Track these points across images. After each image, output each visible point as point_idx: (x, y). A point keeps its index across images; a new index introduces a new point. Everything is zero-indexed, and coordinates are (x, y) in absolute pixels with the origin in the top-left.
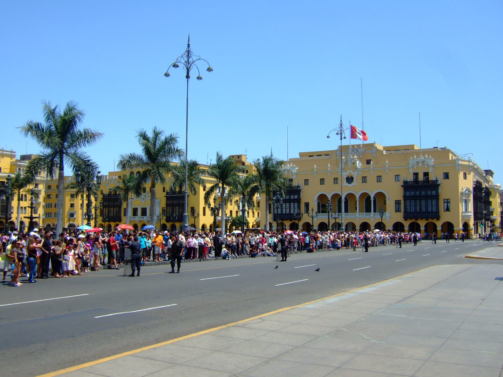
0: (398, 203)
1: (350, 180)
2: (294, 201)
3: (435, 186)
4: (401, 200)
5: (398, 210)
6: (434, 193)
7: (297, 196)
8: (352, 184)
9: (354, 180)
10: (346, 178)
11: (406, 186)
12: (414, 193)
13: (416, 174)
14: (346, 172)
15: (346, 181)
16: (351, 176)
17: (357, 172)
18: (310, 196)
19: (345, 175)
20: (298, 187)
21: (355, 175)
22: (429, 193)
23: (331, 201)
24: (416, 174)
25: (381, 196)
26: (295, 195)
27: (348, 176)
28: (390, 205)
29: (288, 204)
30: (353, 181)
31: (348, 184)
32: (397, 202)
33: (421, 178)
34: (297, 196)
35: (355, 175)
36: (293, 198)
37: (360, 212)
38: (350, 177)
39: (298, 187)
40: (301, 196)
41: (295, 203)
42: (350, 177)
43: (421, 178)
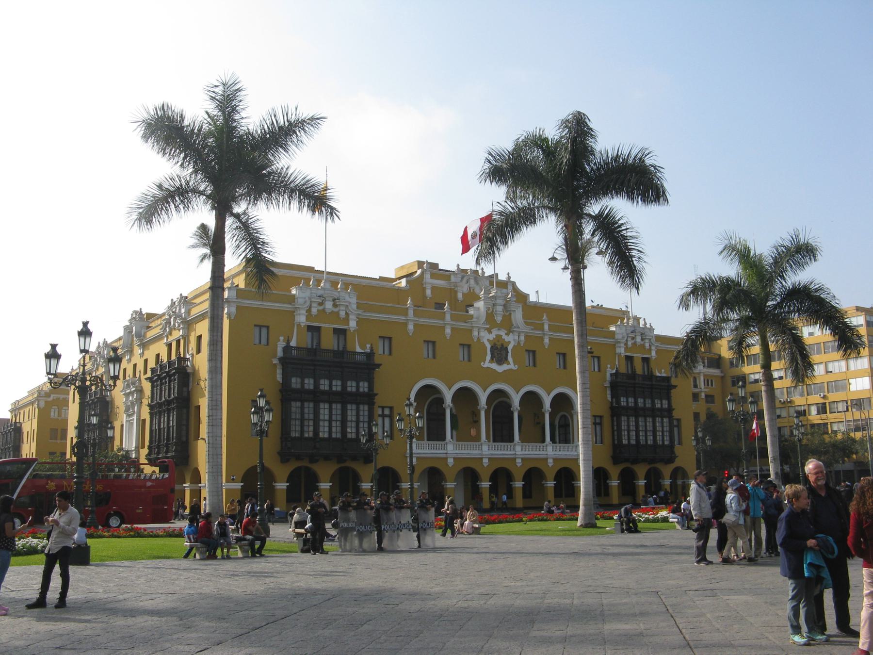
0: (597, 421)
2: (358, 398)
8: (505, 367)
9: (510, 359)
10: (492, 348)
14: (490, 332)
16: (502, 345)
17: (516, 338)
18: (398, 388)
19: (487, 338)
21: (509, 342)
23: (415, 404)
26: (334, 379)
27: (495, 344)
29: (309, 406)
30: (506, 359)
31: (494, 366)
35: (511, 340)
36: (354, 390)
37: (523, 439)
39: (370, 355)
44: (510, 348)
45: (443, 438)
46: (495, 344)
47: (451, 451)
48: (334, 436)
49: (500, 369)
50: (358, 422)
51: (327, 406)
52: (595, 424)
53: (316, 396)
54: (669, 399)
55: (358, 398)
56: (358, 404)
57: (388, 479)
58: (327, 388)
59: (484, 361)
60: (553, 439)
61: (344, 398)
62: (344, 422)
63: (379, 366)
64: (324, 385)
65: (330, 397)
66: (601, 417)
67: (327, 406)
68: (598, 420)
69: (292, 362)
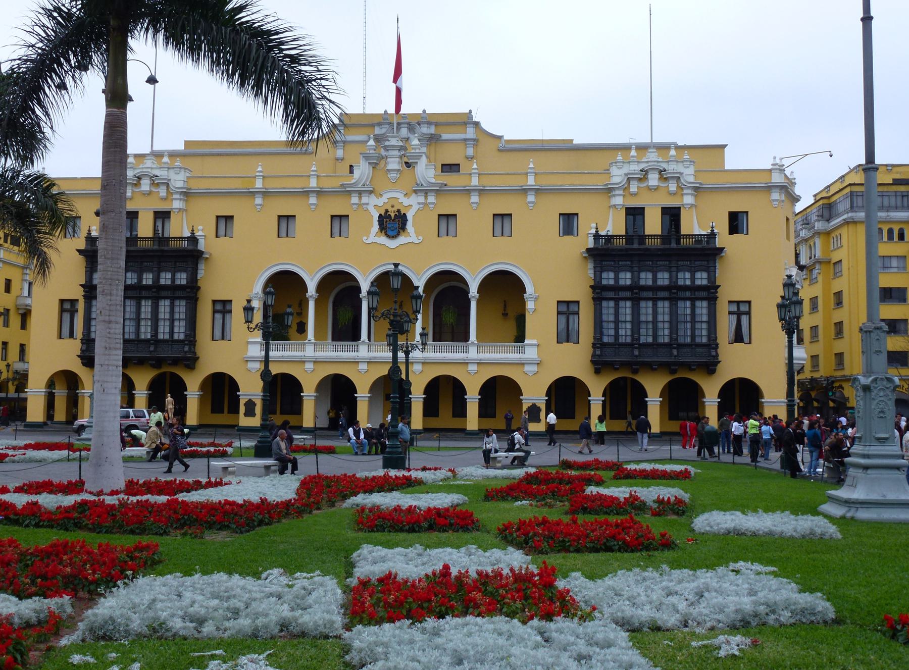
0: (567, 309)
1: (393, 223)
2: (173, 292)
3: (706, 253)
4: (578, 302)
5: (566, 335)
6: (702, 279)
7: (184, 275)
8: (402, 240)
9: (410, 226)
10: (380, 215)
11: (603, 254)
12: (671, 276)
13: (635, 214)
15: (376, 227)
16: (399, 211)
18: (237, 273)
19: (375, 205)
20: (193, 239)
22: (684, 278)
24: (635, 214)
25: (505, 288)
27: (387, 211)
28: (540, 317)
30: (403, 227)
31: (383, 240)
32: (564, 308)
33: (653, 225)
34: (184, 275)
35: (411, 205)
38: (393, 215)
40: (201, 274)
41: (177, 303)
42: (393, 215)
43: (653, 225)
44: (410, 216)
45: (466, 338)
46: (387, 211)
47: (311, 357)
48: (176, 337)
49: (392, 244)
50: (172, 320)
51: (168, 302)
52: (62, 311)
53: (636, 293)
54: (711, 271)
55: (173, 292)
56: (655, 300)
57: (221, 389)
58: (612, 282)
59: (368, 234)
60: (319, 336)
61: (674, 293)
62: (636, 323)
63: (722, 249)
64: (646, 279)
65: (655, 293)
66: (73, 302)
67: (168, 302)
68: (67, 306)
69: (603, 254)
